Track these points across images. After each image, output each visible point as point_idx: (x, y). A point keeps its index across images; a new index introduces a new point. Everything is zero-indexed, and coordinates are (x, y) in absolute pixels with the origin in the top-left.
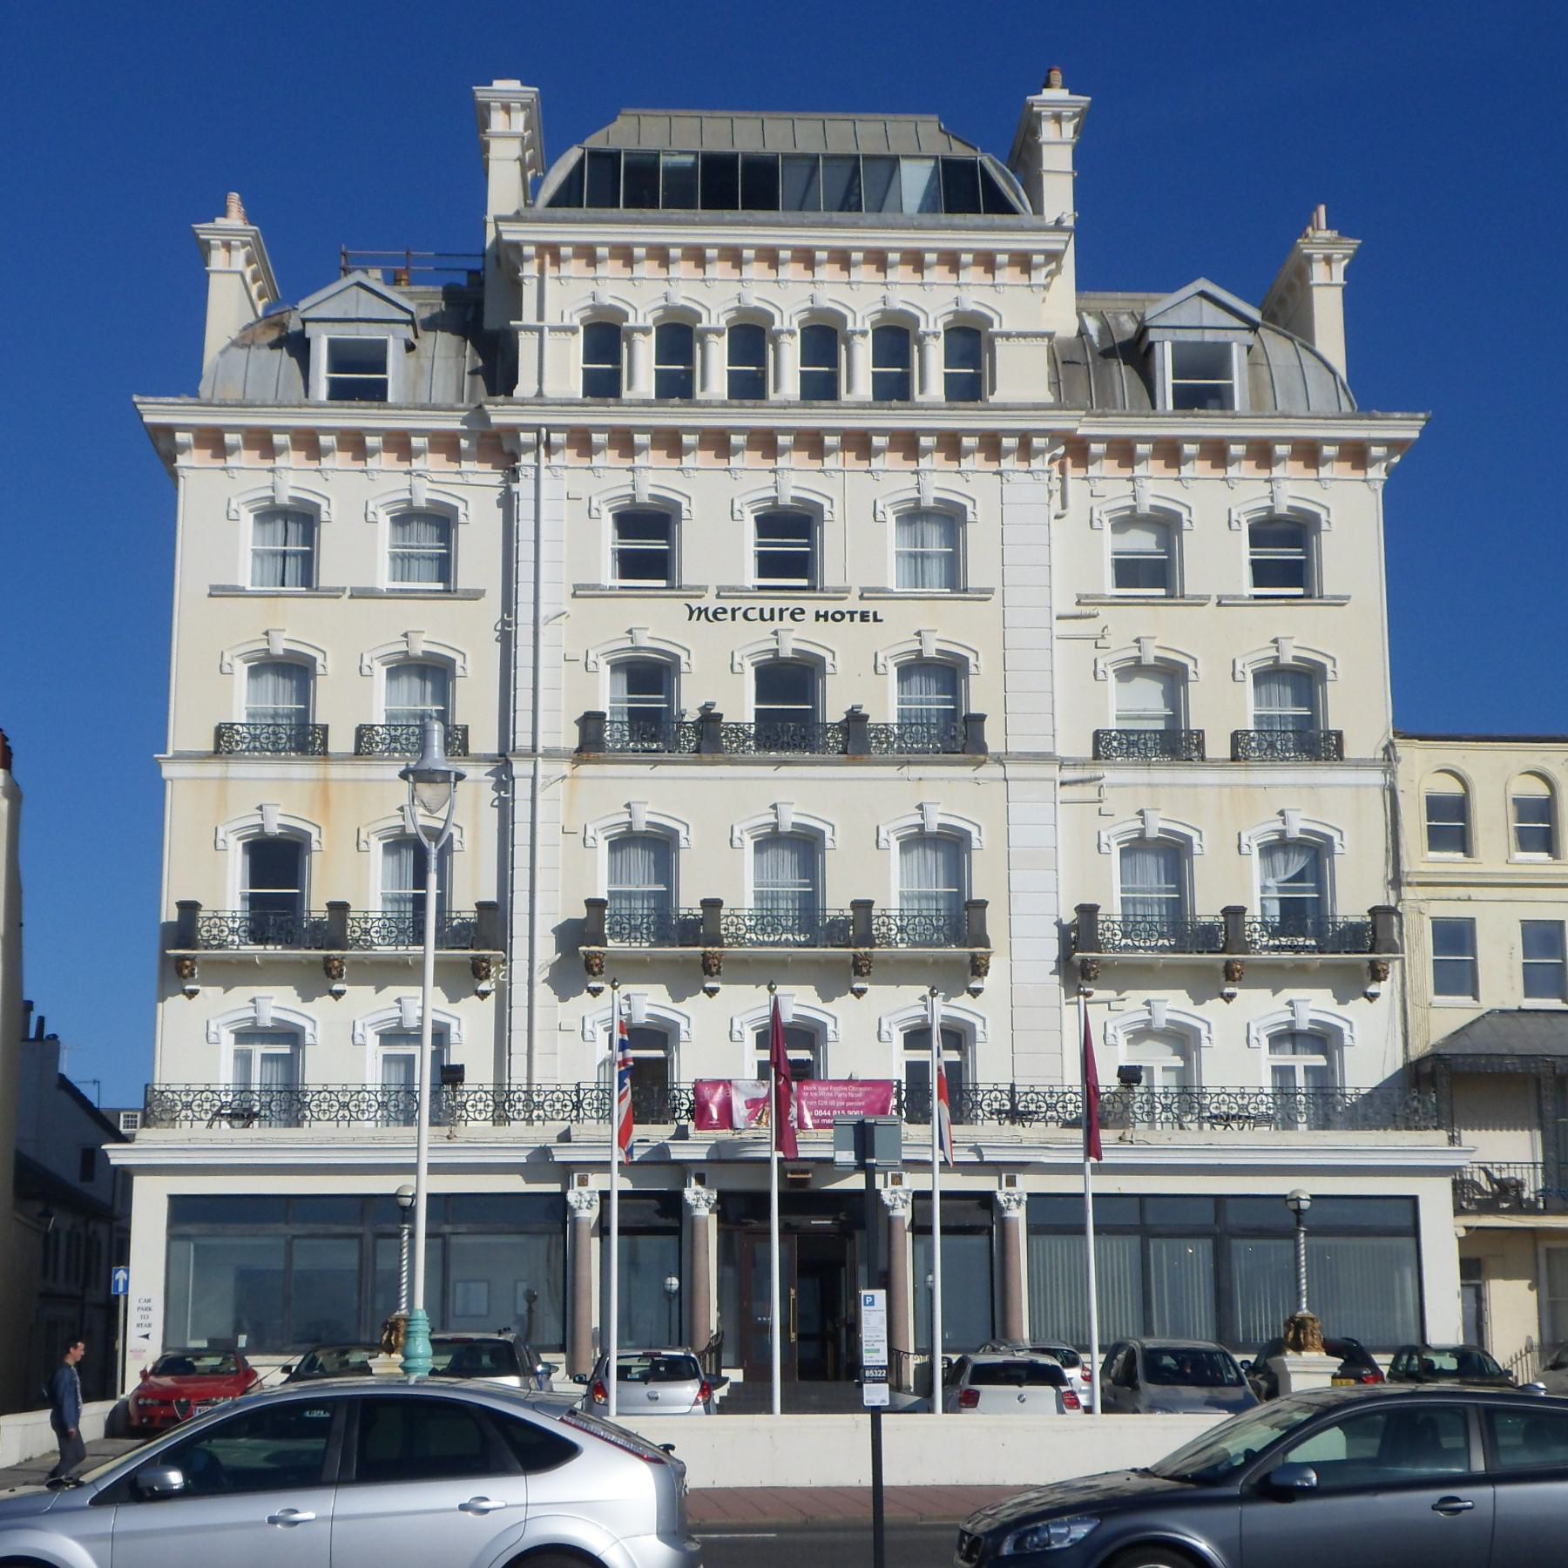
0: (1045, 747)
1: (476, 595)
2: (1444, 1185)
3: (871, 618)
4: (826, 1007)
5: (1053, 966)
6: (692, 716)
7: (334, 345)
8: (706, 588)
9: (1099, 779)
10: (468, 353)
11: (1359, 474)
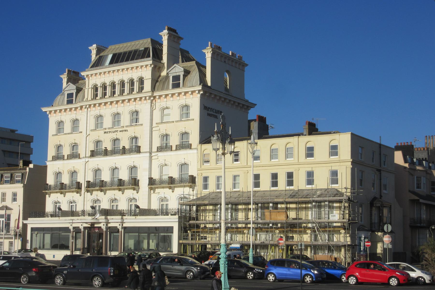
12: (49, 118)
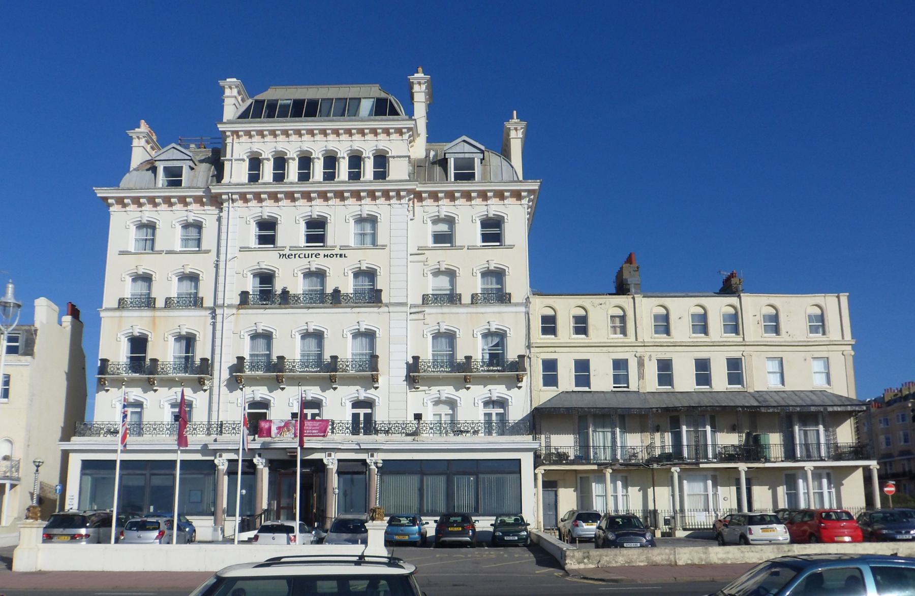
0: (403, 300)
1: (207, 252)
2: (531, 455)
3: (343, 256)
4: (323, 394)
5: (404, 378)
6: (279, 291)
7: (165, 168)
8: (285, 247)
9: (424, 311)
10: (212, 170)
11: (519, 202)
12: (112, 213)
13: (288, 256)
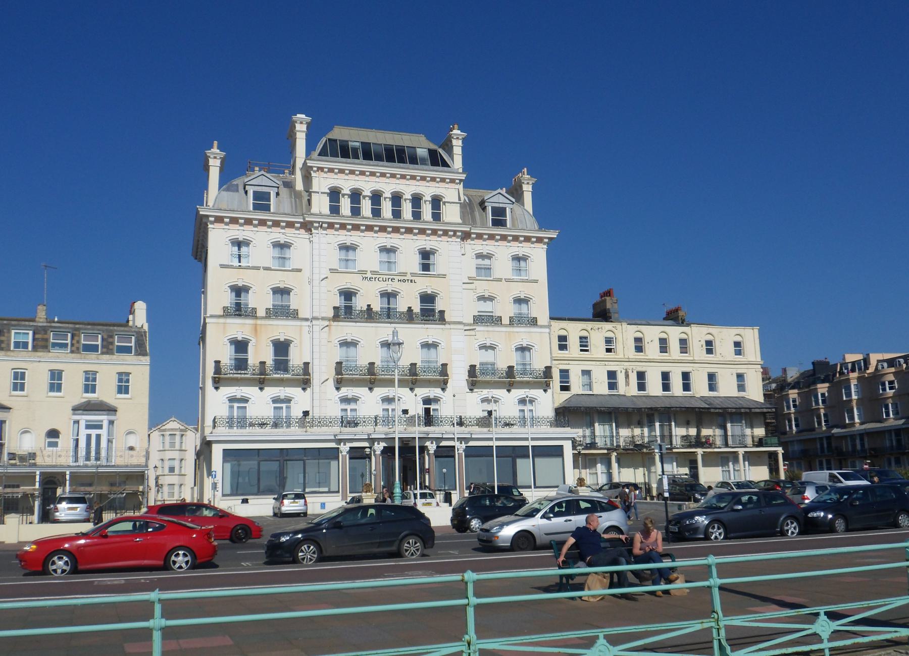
7: (255, 193)
13: (370, 279)
